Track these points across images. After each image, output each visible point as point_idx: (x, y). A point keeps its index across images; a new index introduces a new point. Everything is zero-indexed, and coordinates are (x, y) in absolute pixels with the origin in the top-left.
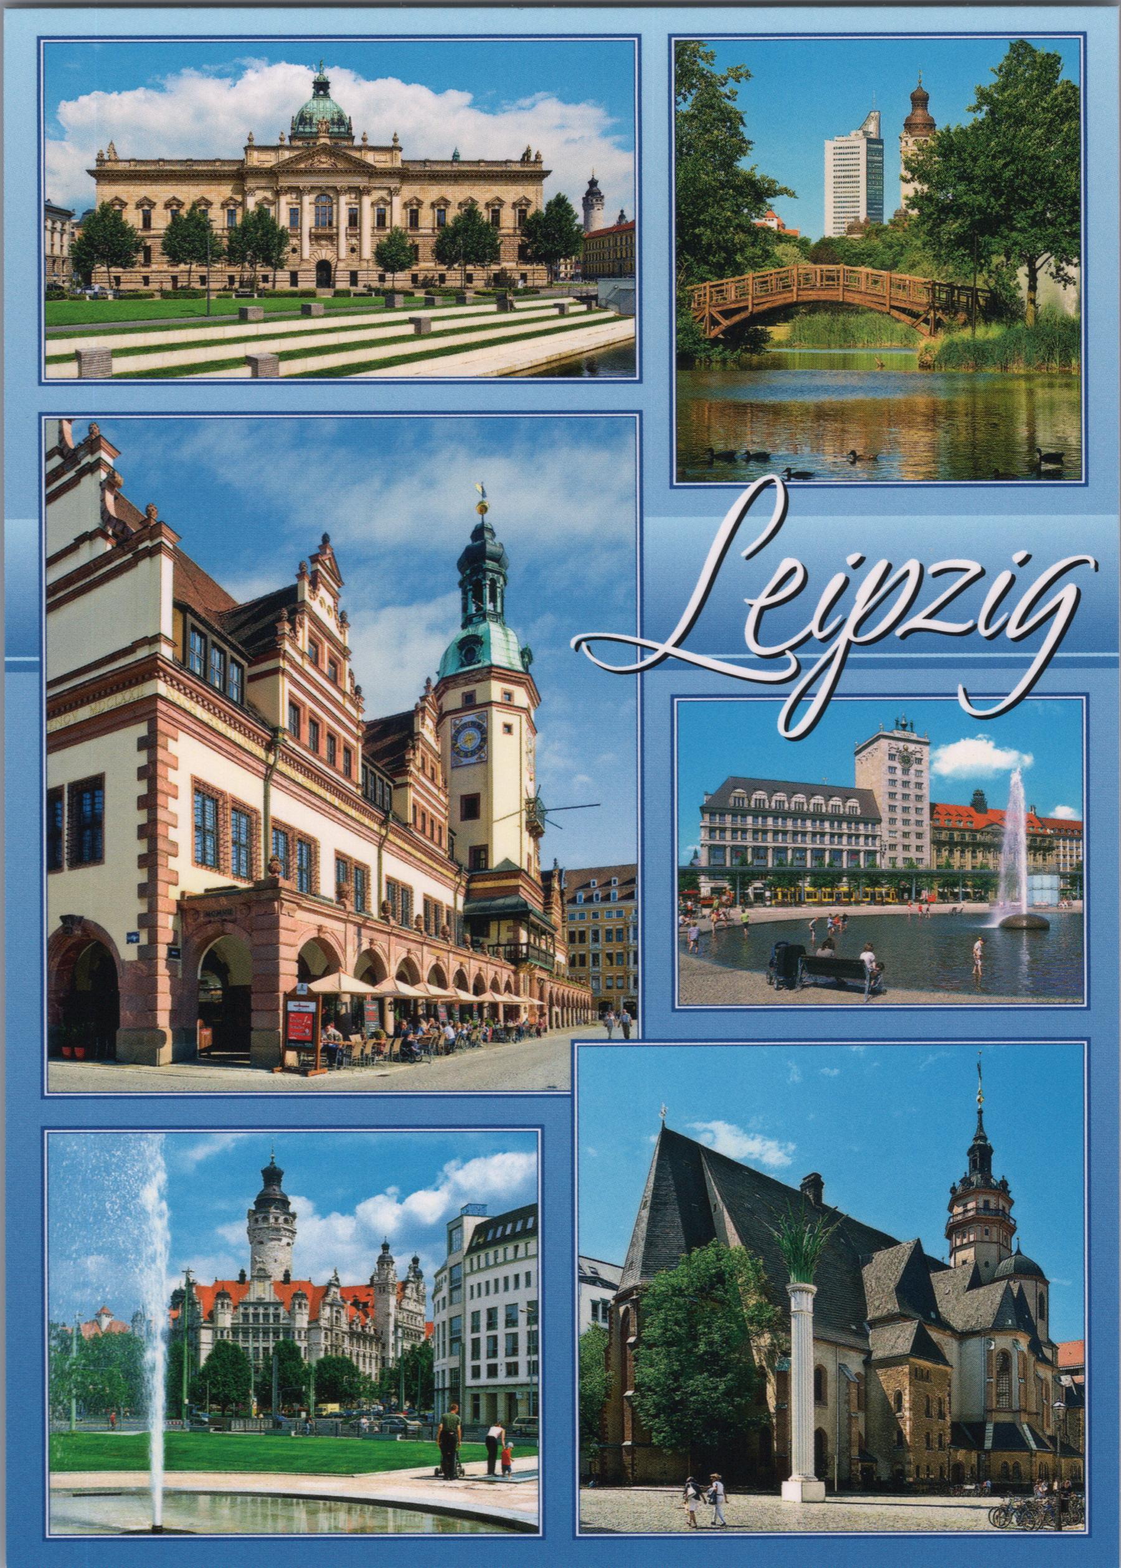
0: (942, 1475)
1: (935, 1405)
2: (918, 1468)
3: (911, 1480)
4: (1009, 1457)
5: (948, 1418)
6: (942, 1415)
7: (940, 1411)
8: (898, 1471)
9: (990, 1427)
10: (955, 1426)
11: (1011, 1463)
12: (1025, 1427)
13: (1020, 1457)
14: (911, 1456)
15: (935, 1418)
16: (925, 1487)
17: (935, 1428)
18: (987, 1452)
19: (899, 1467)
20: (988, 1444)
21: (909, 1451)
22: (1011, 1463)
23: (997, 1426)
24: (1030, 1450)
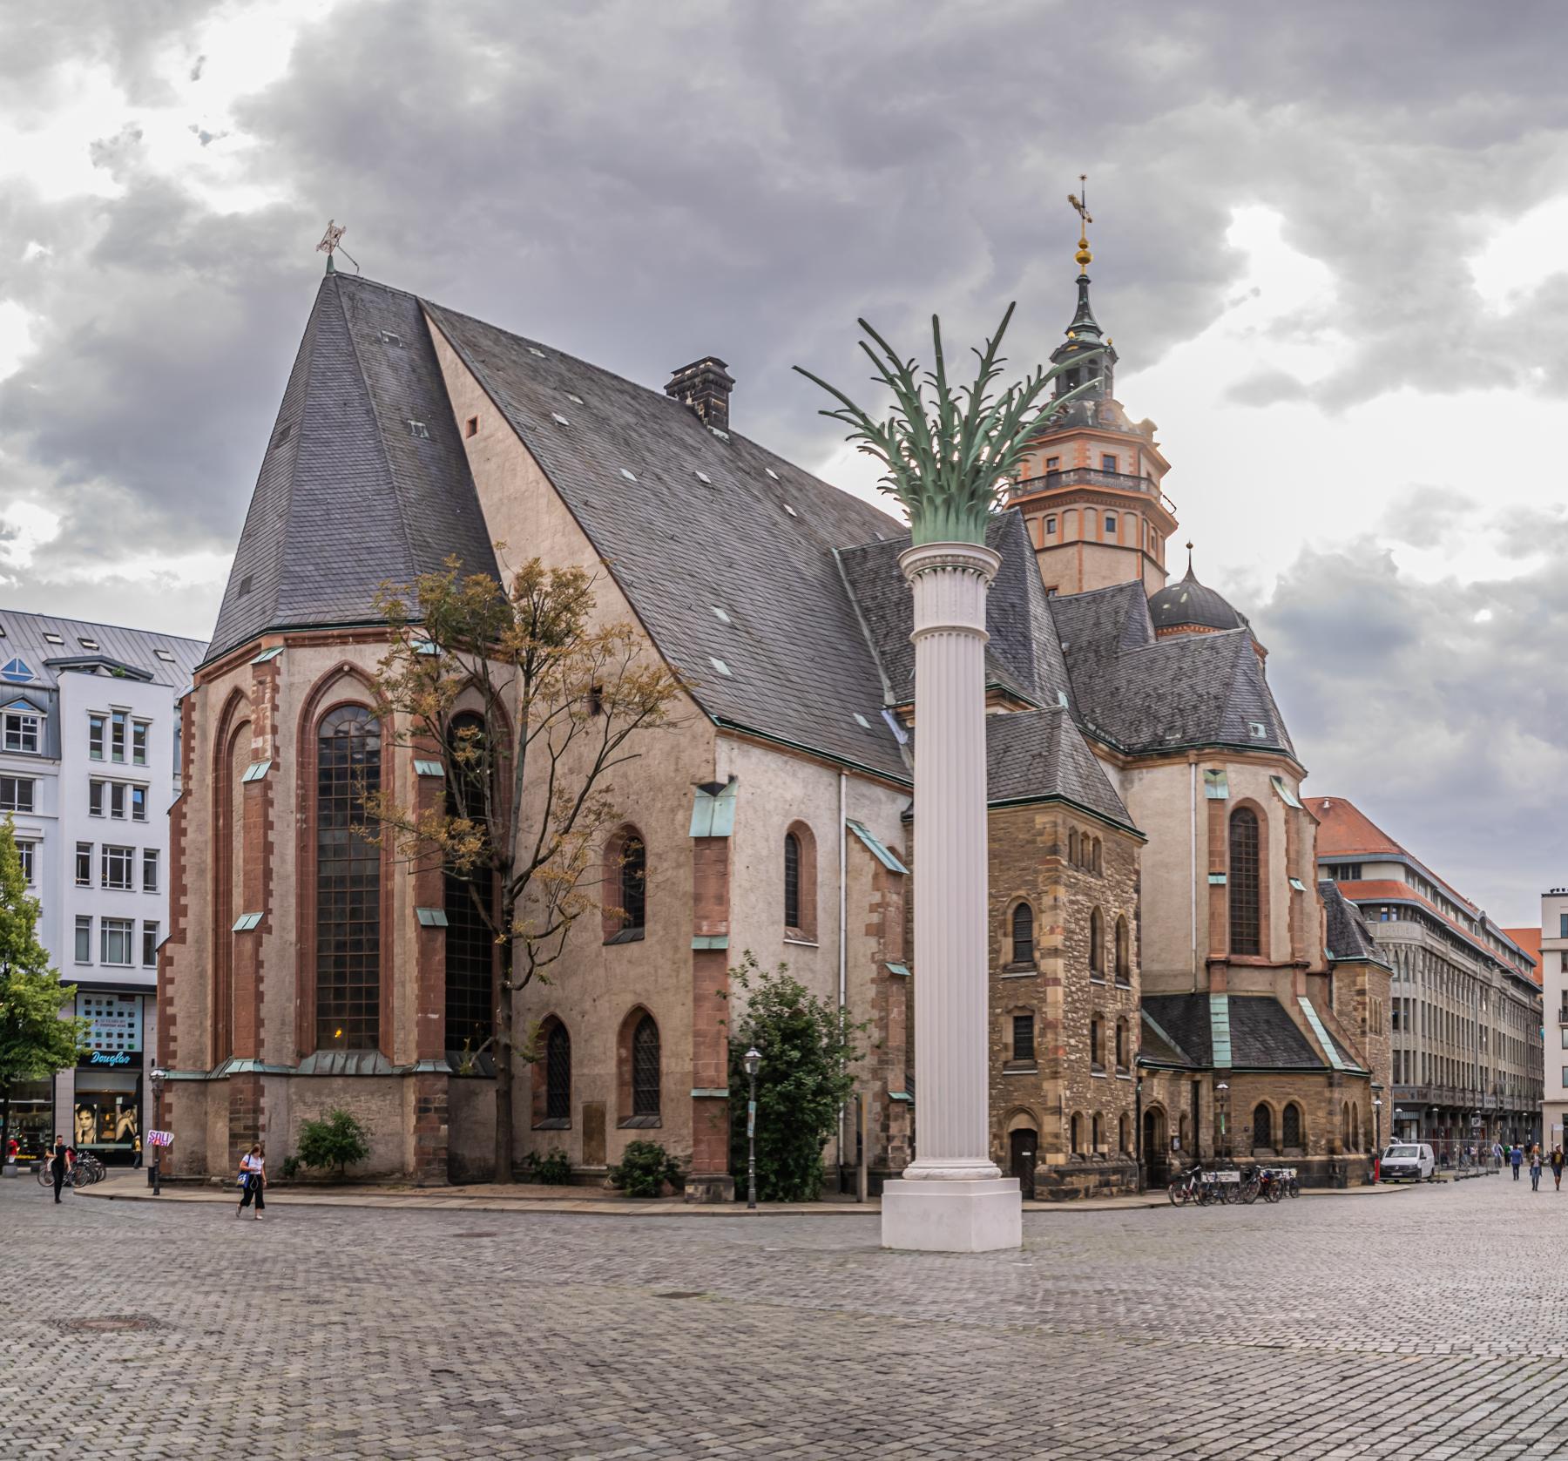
0: (1123, 1148)
1: (1109, 939)
2: (1075, 1120)
3: (1059, 1159)
4: (1276, 1094)
5: (1135, 981)
6: (1122, 973)
7: (1118, 958)
8: (1018, 1135)
9: (1219, 1006)
10: (1147, 1002)
11: (1278, 1107)
12: (1305, 1003)
13: (1303, 1091)
14: (1057, 1090)
15: (1109, 980)
16: (1093, 1180)
17: (1111, 1008)
18: (1220, 1074)
19: (1021, 1122)
20: (1223, 1055)
21: (1055, 1075)
22: (1278, 1107)
23: (1233, 1001)
24: (1326, 1071)
